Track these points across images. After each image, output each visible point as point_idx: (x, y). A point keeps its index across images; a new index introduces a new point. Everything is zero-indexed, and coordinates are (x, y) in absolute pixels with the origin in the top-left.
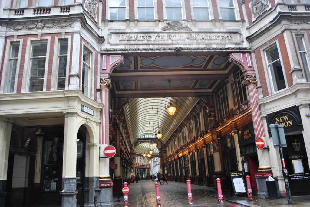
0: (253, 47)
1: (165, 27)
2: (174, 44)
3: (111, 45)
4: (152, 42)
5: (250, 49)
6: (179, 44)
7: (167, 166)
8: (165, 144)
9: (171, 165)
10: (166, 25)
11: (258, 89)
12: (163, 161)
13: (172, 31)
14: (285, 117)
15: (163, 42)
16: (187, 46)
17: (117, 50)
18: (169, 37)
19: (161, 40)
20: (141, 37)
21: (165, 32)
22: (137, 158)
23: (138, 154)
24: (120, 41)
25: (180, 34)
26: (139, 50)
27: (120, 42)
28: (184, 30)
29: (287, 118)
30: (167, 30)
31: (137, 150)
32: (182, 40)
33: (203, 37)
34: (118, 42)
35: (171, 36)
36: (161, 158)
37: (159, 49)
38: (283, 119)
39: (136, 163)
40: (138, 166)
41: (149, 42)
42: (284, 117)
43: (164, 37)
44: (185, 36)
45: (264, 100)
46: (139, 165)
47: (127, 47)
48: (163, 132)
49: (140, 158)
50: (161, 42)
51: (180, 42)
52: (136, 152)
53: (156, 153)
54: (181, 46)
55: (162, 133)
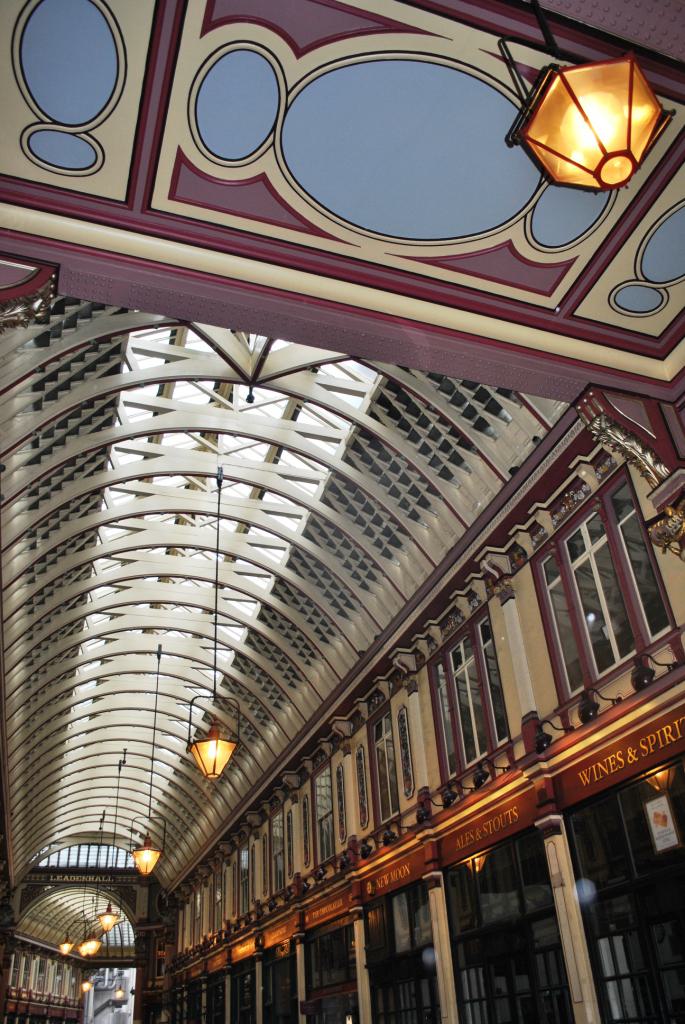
7: (172, 1005)
8: (178, 888)
9: (204, 996)
12: (150, 984)
22: (28, 967)
23: (34, 948)
31: (34, 924)
36: (143, 966)
39: (19, 991)
40: (27, 1006)
46: (31, 1000)
48: (168, 841)
49: (42, 969)
52: (26, 936)
53: (115, 948)
55: (164, 843)
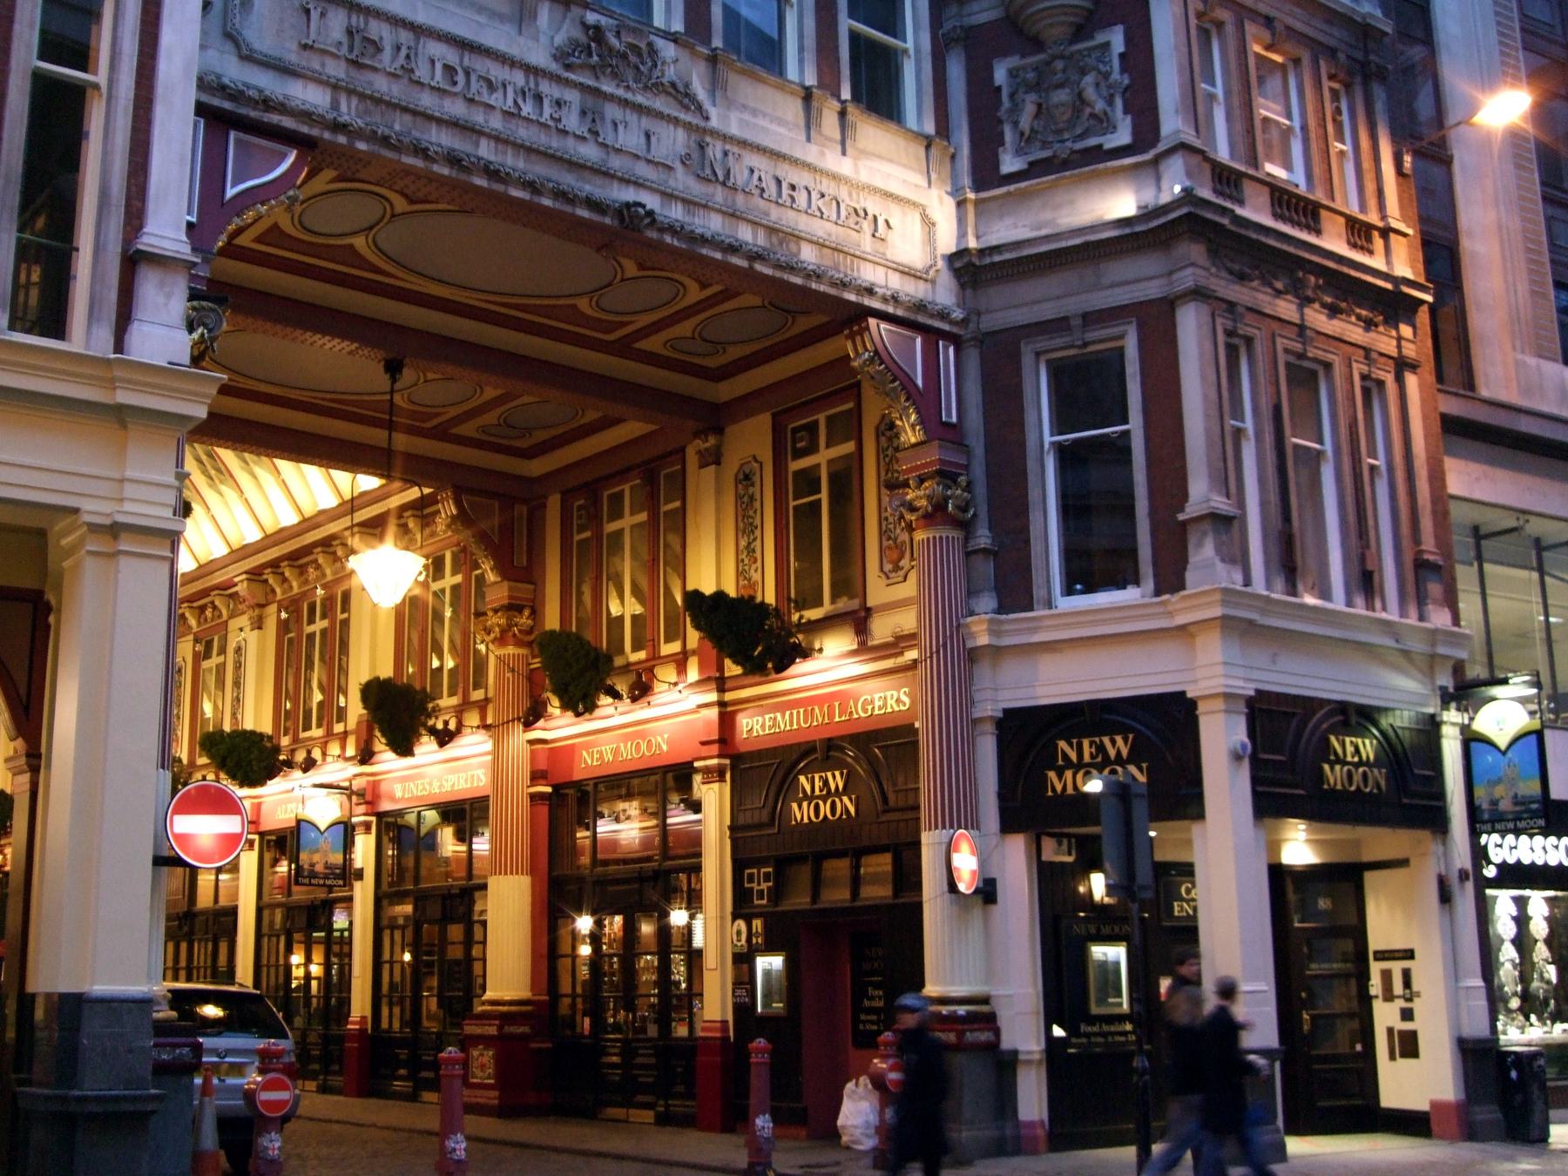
0: (979, 314)
1: (575, 45)
2: (613, 177)
3: (249, 57)
4: (496, 123)
5: (964, 322)
6: (638, 184)
10: (578, 34)
11: (973, 557)
13: (608, 87)
14: (1113, 742)
15: (555, 143)
16: (676, 213)
17: (282, 108)
18: (594, 121)
19: (548, 126)
20: (438, 66)
21: (572, 76)
24: (305, 47)
25: (646, 122)
26: (421, 151)
27: (306, 54)
28: (670, 99)
29: (1125, 752)
30: (582, 67)
32: (657, 164)
33: (760, 179)
34: (293, 57)
35: (603, 119)
37: (530, 186)
38: (1101, 749)
41: (478, 117)
42: (1106, 740)
43: (565, 110)
44: (671, 142)
45: (1007, 627)
47: (348, 110)
50: (541, 139)
51: (643, 170)
54: (651, 201)
